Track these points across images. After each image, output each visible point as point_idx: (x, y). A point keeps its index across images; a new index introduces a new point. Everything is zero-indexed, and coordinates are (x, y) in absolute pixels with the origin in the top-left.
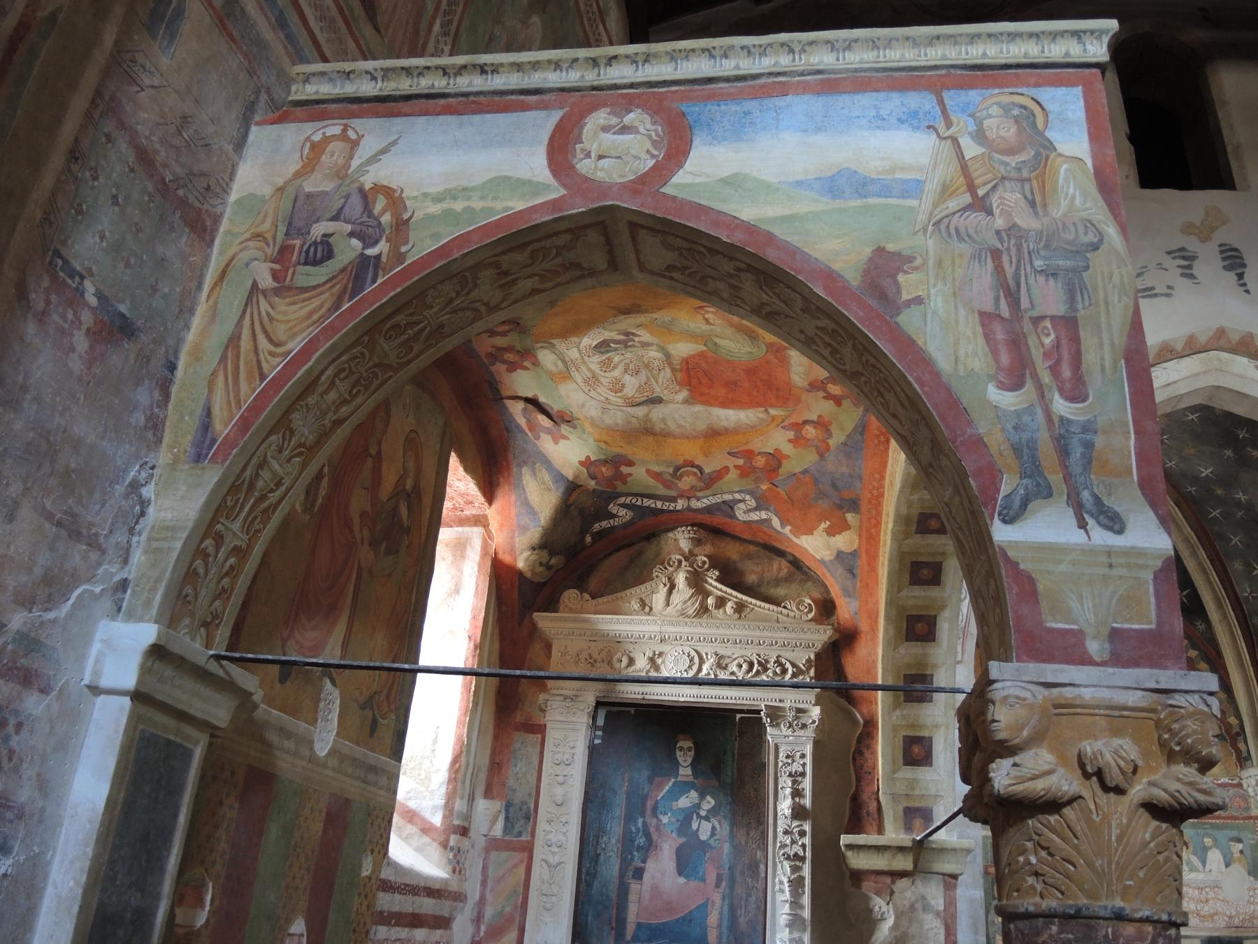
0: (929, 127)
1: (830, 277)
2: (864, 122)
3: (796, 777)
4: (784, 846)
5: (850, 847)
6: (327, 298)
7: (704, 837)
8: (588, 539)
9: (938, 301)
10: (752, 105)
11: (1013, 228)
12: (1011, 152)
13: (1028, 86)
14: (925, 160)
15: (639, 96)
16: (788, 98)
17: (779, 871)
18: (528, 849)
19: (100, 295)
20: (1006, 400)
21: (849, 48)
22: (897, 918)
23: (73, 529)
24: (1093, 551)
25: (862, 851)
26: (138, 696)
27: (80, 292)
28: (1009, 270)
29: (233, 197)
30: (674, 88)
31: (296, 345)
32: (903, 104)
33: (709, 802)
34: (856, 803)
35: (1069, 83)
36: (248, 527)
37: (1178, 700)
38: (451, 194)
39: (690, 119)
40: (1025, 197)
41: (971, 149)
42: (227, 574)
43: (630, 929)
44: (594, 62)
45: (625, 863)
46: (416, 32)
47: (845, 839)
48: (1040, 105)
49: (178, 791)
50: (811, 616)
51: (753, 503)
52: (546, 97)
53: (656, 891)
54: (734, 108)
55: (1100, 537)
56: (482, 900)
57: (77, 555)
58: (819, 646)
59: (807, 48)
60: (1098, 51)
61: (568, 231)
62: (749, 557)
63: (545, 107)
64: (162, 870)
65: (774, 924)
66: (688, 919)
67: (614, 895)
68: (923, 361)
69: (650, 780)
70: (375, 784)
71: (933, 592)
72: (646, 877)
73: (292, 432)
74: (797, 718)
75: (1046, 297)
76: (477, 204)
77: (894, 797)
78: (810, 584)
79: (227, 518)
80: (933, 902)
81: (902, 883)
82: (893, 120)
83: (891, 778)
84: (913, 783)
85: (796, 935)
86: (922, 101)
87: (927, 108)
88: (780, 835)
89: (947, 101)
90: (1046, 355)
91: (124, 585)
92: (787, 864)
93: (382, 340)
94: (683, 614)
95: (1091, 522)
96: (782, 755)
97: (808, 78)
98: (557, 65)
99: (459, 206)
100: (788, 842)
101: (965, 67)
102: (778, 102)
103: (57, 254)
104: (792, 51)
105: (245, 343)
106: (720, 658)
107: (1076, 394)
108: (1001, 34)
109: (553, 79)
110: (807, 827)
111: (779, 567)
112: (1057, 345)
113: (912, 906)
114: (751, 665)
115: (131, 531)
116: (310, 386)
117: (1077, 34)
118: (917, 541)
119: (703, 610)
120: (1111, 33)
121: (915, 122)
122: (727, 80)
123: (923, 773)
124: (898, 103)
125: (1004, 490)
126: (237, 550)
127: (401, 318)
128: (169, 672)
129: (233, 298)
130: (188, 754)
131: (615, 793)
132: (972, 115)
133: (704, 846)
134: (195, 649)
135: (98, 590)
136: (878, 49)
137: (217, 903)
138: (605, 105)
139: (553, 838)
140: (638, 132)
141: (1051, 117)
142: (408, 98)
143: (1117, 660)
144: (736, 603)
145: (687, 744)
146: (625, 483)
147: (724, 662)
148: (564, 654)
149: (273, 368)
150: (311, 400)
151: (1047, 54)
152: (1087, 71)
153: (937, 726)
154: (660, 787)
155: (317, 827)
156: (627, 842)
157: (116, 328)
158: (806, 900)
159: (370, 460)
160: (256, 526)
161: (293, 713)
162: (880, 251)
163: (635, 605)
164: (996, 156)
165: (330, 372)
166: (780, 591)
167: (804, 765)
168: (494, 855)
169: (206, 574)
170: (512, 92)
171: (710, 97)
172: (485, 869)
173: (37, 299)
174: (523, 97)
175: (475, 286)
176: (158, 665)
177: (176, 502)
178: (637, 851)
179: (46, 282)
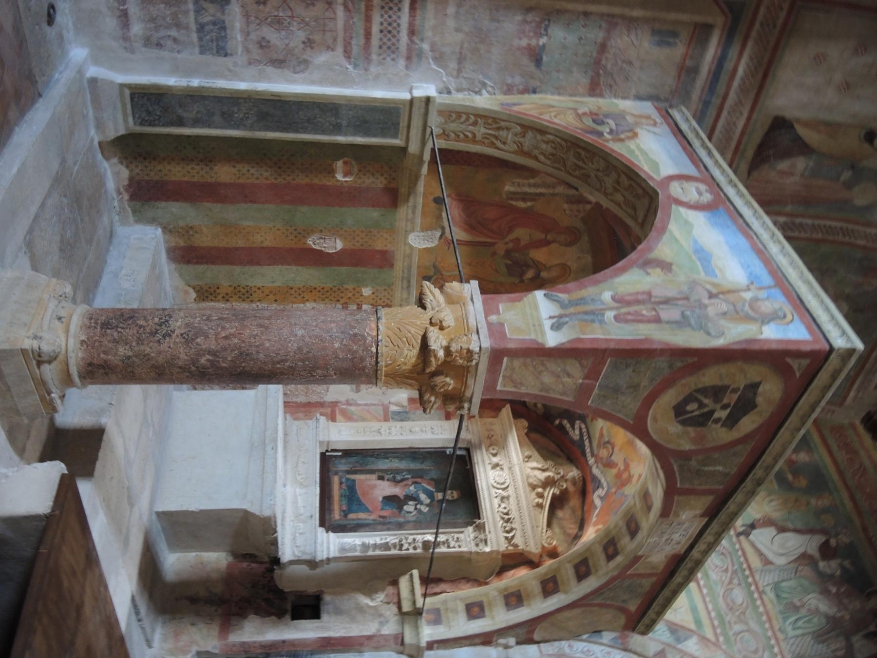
1: (650, 249)
3: (446, 543)
4: (407, 539)
5: (411, 575)
6: (580, 126)
7: (405, 508)
8: (557, 422)
9: (648, 279)
11: (706, 307)
12: (751, 307)
17: (392, 538)
18: (386, 419)
19: (544, 46)
20: (607, 296)
22: (374, 607)
23: (461, 60)
24: (539, 319)
25: (410, 585)
26: (412, 101)
27: (541, 36)
28: (680, 302)
29: (616, 101)
31: (556, 120)
33: (425, 509)
34: (439, 580)
36: (486, 137)
37: (475, 337)
38: (642, 151)
41: (748, 296)
42: (465, 135)
43: (353, 477)
45: (386, 471)
47: (415, 573)
49: (384, 136)
50: (546, 545)
51: (603, 494)
53: (374, 486)
55: (547, 324)
56: (359, 405)
57: (453, 65)
58: (528, 549)
61: (644, 190)
62: (574, 511)
64: (355, 135)
65: (362, 537)
66: (360, 503)
67: (369, 467)
68: (617, 274)
69: (432, 479)
70: (402, 288)
71: (573, 580)
72: (380, 482)
73: (524, 136)
74: (481, 540)
75: (669, 314)
76: (641, 158)
77: (445, 602)
78: (566, 545)
79: (485, 123)
80: (385, 628)
81: (394, 609)
83: (455, 599)
84: (455, 611)
85: (358, 548)
88: (412, 537)
90: (636, 312)
91: (449, 92)
92: (397, 541)
93: (572, 153)
94: (528, 477)
95: (554, 320)
96: (456, 536)
99: (637, 152)
100: (409, 541)
103: (549, 21)
105: (551, 109)
106: (508, 498)
107: (616, 318)
110: (419, 551)
111: (573, 529)
112: (643, 315)
113: (381, 615)
114: (507, 514)
115: (469, 90)
116: (541, 131)
117: (844, 333)
118: (599, 549)
119: (533, 487)
123: (462, 616)
125: (560, 295)
126: (474, 135)
127: (583, 153)
128: (423, 110)
129: (571, 105)
130: (395, 136)
131: (422, 463)
133: (400, 508)
134: (435, 121)
135: (444, 79)
137: (345, 184)
139: (393, 429)
143: (490, 325)
144: (542, 504)
145: (455, 495)
146: (592, 420)
147: (505, 500)
148: (491, 424)
149: (546, 117)
150: (539, 137)
153: (493, 618)
154: (428, 484)
155: (379, 246)
156: (398, 471)
157: (536, 56)
158: (378, 552)
159: (543, 236)
160: (486, 141)
161: (423, 213)
162: (671, 264)
163: (527, 453)
165: (551, 137)
166: (557, 529)
167: (454, 547)
168: (381, 408)
169: (462, 123)
172: (375, 405)
173: (530, 17)
175: (608, 175)
176: (423, 104)
177: (484, 101)
178: (394, 477)
179: (537, 19)
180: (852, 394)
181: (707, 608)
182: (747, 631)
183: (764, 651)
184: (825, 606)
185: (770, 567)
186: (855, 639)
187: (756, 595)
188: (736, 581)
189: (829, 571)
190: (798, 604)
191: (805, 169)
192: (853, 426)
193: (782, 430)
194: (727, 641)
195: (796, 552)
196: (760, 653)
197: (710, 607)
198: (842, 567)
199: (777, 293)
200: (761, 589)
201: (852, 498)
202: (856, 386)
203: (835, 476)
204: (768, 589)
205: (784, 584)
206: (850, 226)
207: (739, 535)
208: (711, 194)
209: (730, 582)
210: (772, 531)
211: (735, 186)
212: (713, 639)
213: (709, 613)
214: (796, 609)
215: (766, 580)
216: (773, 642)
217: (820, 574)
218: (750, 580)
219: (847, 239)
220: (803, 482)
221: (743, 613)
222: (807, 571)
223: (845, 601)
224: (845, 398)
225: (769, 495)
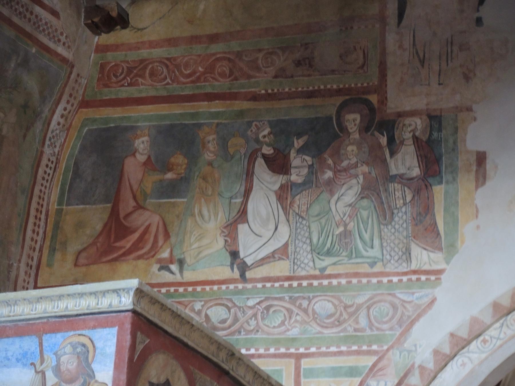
0: (32, 364)
13: (89, 328)
32: (20, 347)
35: (112, 326)
48: (92, 342)
60: (127, 302)
82: (14, 360)
86: (29, 344)
87: (33, 349)
89: (45, 344)
101: (56, 317)
108: (75, 294)
120: (134, 290)
121: (24, 361)
132: (55, 354)
136: (11, 306)
141: (97, 352)
151: (99, 306)
152: (123, 314)
180: (60, 50)
181: (334, 354)
182: (369, 308)
183: (394, 295)
184: (348, 194)
185: (291, 249)
186: (394, 171)
187: (325, 282)
188: (305, 304)
189: (305, 171)
190: (341, 229)
192: (101, 49)
193: (190, 343)
194: (378, 340)
195: (274, 206)
196: (397, 301)
197: (333, 349)
198: (299, 151)
199: (52, 340)
200: (317, 273)
201: (210, 97)
202: (51, 45)
203: (176, 109)
204: (320, 264)
205: (315, 240)
207: (243, 275)
209: (305, 311)
210: (242, 228)
212: (374, 358)
213: (340, 353)
214: (347, 234)
215: (308, 264)
216: (385, 280)
217: (307, 184)
218: (305, 283)
220: (179, 159)
221: (346, 307)
222: (301, 200)
223: (345, 164)
224: (64, 60)
225: (193, 215)
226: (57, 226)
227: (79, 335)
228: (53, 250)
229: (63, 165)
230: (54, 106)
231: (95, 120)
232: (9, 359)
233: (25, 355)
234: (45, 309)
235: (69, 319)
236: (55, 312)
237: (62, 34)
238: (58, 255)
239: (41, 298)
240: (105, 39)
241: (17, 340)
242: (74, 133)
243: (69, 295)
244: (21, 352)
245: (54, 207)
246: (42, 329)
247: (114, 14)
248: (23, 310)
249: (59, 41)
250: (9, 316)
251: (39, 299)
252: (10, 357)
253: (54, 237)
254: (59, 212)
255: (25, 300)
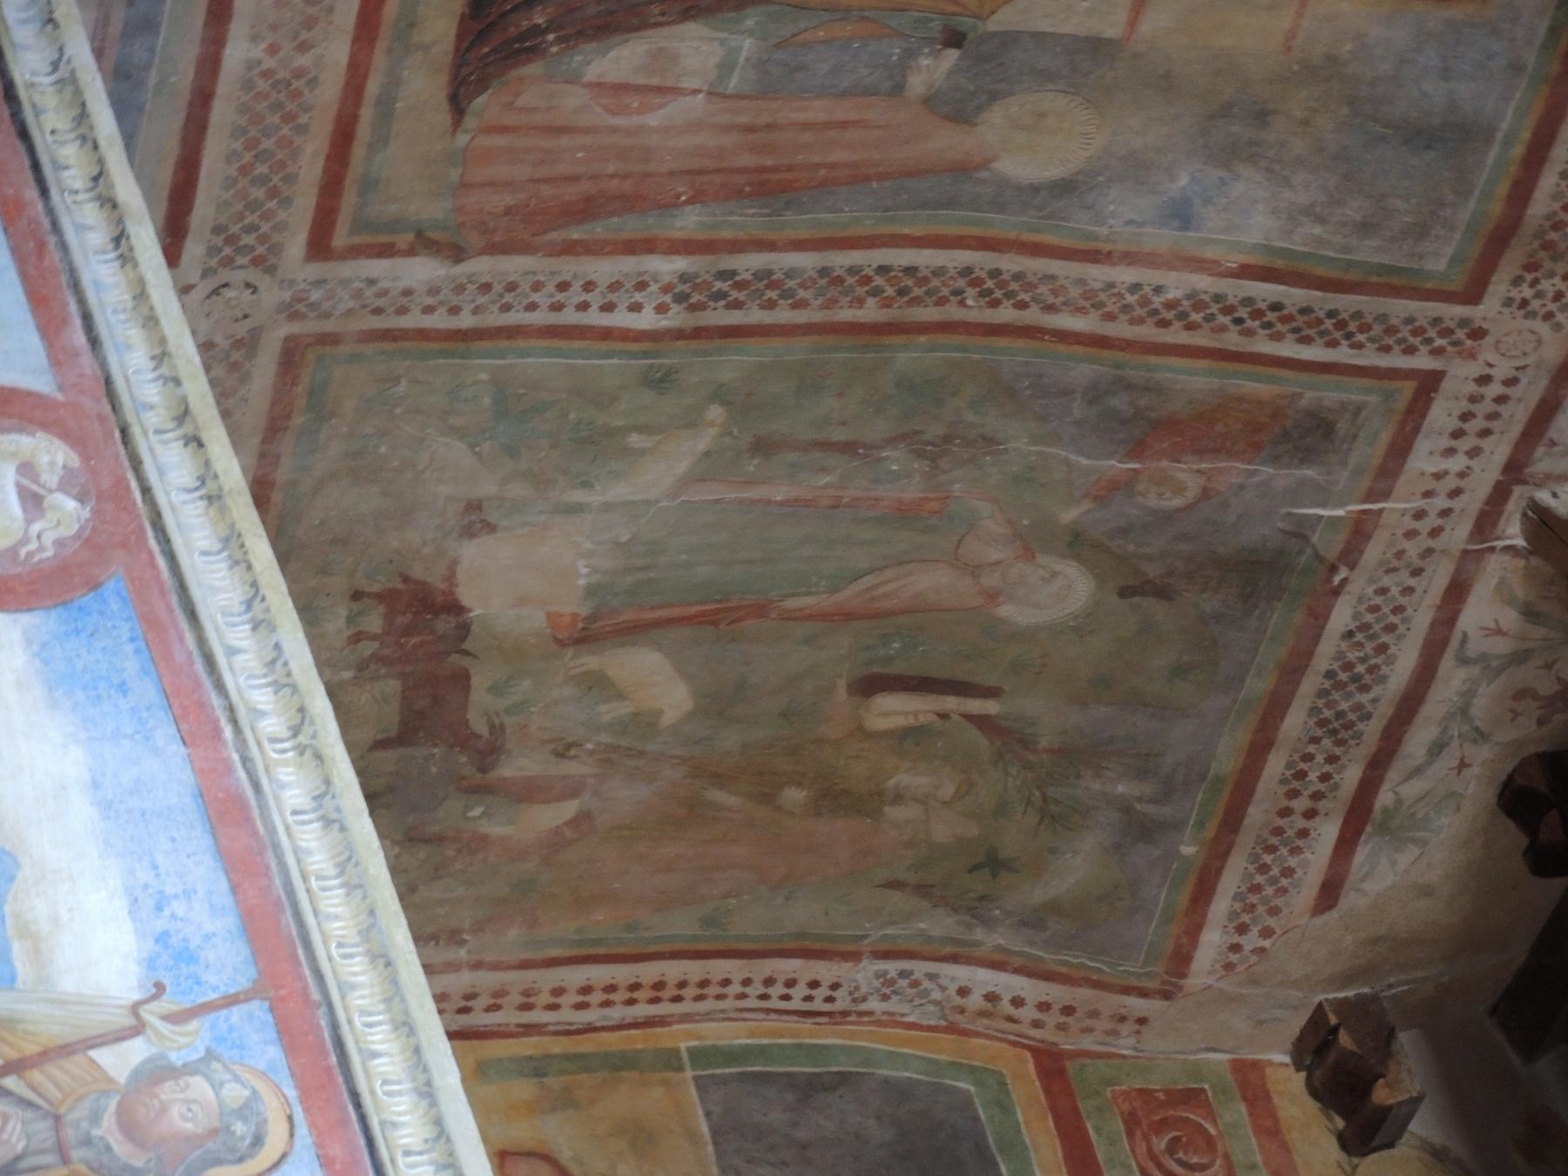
0: (160, 987)
2: (143, 875)
10: (147, 691)
12: (129, 1126)
13: (319, 1145)
14: (68, 985)
15: (130, 508)
16: (177, 750)
21: (327, 822)
30: (161, 562)
32: (208, 937)
39: (88, 600)
40: (18, 1158)
41: (120, 1061)
44: (183, 414)
46: (586, 210)
52: (87, 360)
54: (131, 666)
59: (309, 753)
63: (58, 358)
82: (160, 925)
86: (226, 961)
87: (211, 978)
89: (236, 1014)
97: (242, 775)
98: (161, 356)
101: (335, 1027)
102: (165, 733)
104: (296, 731)
108: (425, 1070)
109: (131, 361)
122: (202, 641)
124: (209, 927)
132: (210, 1055)
136: (341, 874)
138: (85, 457)
140: (29, 521)
142: (24, 135)
151: (401, 1161)
164: (112, 1105)
170: (82, 301)
171: (154, 632)
174: (77, 322)
180: (1213, 939)
191: (726, 67)
192: (1250, 1081)
199: (253, 1028)
202: (1221, 905)
206: (1009, 263)
208: (81, 499)
211: (195, 441)
219: (1006, 314)
224: (1181, 961)
226: (621, 1063)
227: (290, 1118)
228: (536, 1068)
229: (830, 1038)
230: (1017, 961)
231: (1004, 1106)
232: (159, 908)
233: (186, 956)
234: (354, 987)
235: (337, 1071)
236: (350, 1022)
237: (1267, 933)
238: (524, 1089)
239: (388, 964)
240: (1290, 1089)
241: (230, 921)
242: (944, 1050)
243: (417, 1050)
244: (193, 945)
245: (682, 1039)
246: (283, 992)
247: (1381, 1095)
248: (336, 917)
249: (1242, 929)
250: (305, 878)
251: (383, 960)
252: (167, 912)
253: (582, 1062)
254: (669, 1060)
255: (372, 913)
